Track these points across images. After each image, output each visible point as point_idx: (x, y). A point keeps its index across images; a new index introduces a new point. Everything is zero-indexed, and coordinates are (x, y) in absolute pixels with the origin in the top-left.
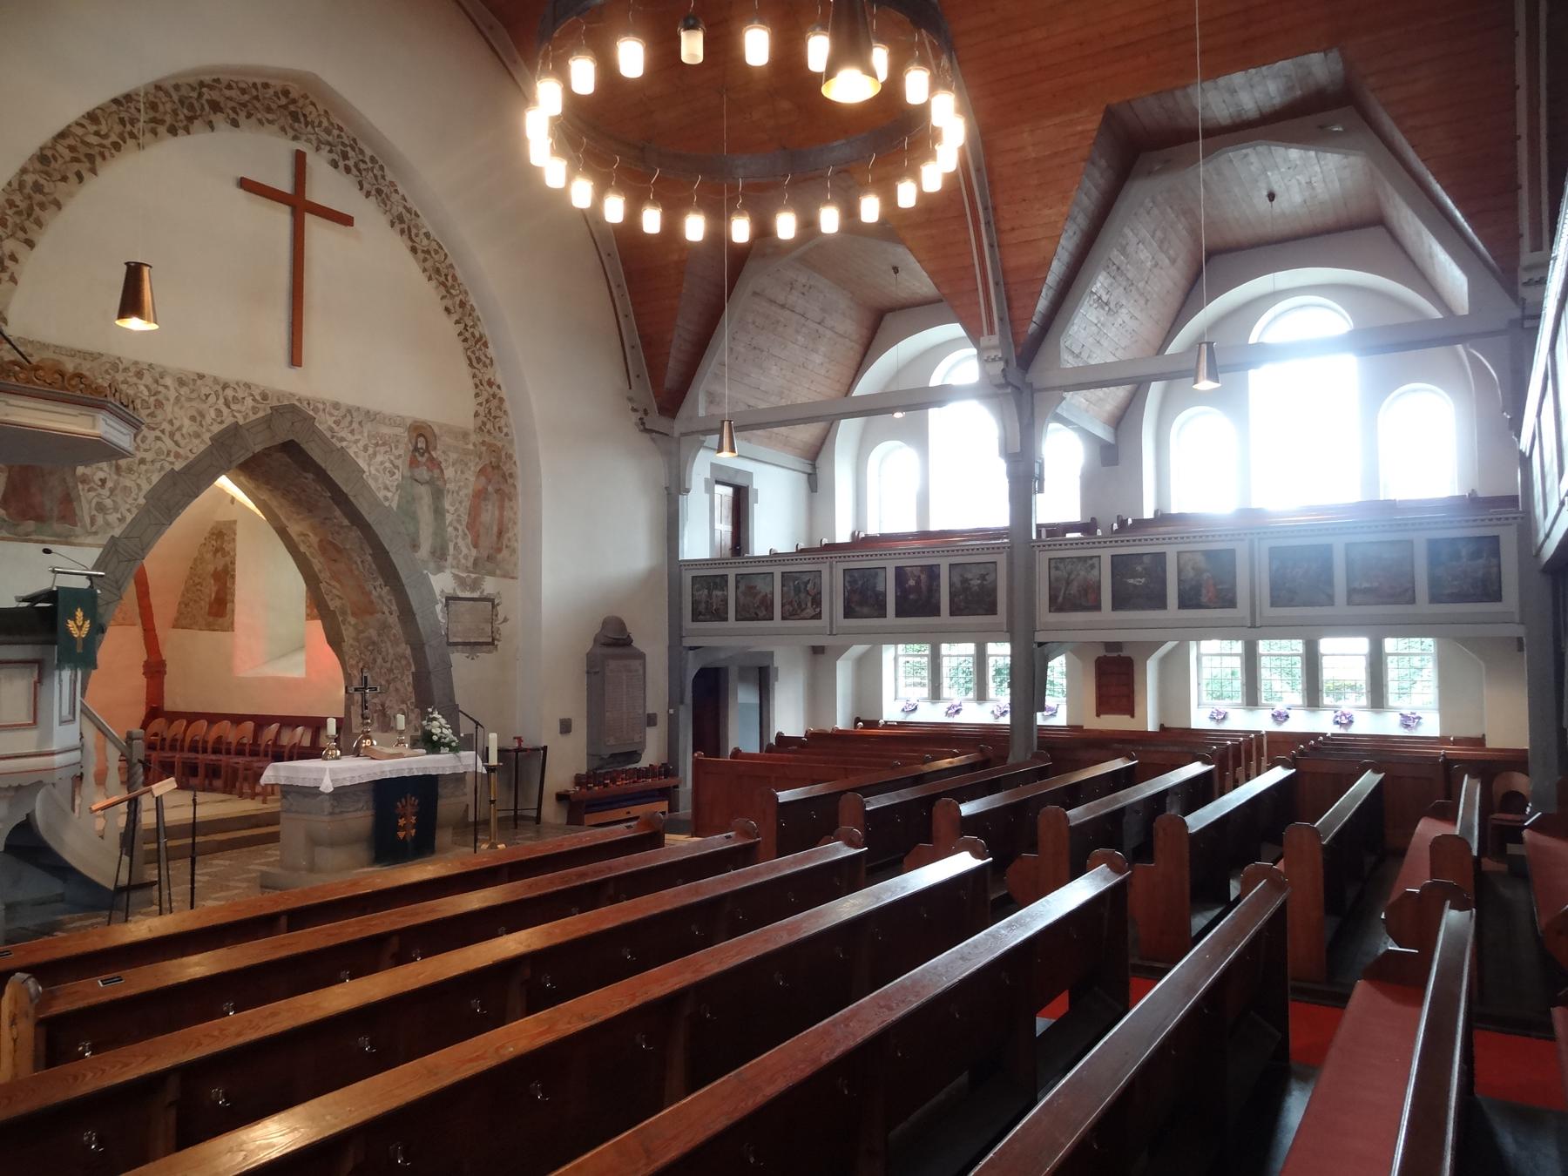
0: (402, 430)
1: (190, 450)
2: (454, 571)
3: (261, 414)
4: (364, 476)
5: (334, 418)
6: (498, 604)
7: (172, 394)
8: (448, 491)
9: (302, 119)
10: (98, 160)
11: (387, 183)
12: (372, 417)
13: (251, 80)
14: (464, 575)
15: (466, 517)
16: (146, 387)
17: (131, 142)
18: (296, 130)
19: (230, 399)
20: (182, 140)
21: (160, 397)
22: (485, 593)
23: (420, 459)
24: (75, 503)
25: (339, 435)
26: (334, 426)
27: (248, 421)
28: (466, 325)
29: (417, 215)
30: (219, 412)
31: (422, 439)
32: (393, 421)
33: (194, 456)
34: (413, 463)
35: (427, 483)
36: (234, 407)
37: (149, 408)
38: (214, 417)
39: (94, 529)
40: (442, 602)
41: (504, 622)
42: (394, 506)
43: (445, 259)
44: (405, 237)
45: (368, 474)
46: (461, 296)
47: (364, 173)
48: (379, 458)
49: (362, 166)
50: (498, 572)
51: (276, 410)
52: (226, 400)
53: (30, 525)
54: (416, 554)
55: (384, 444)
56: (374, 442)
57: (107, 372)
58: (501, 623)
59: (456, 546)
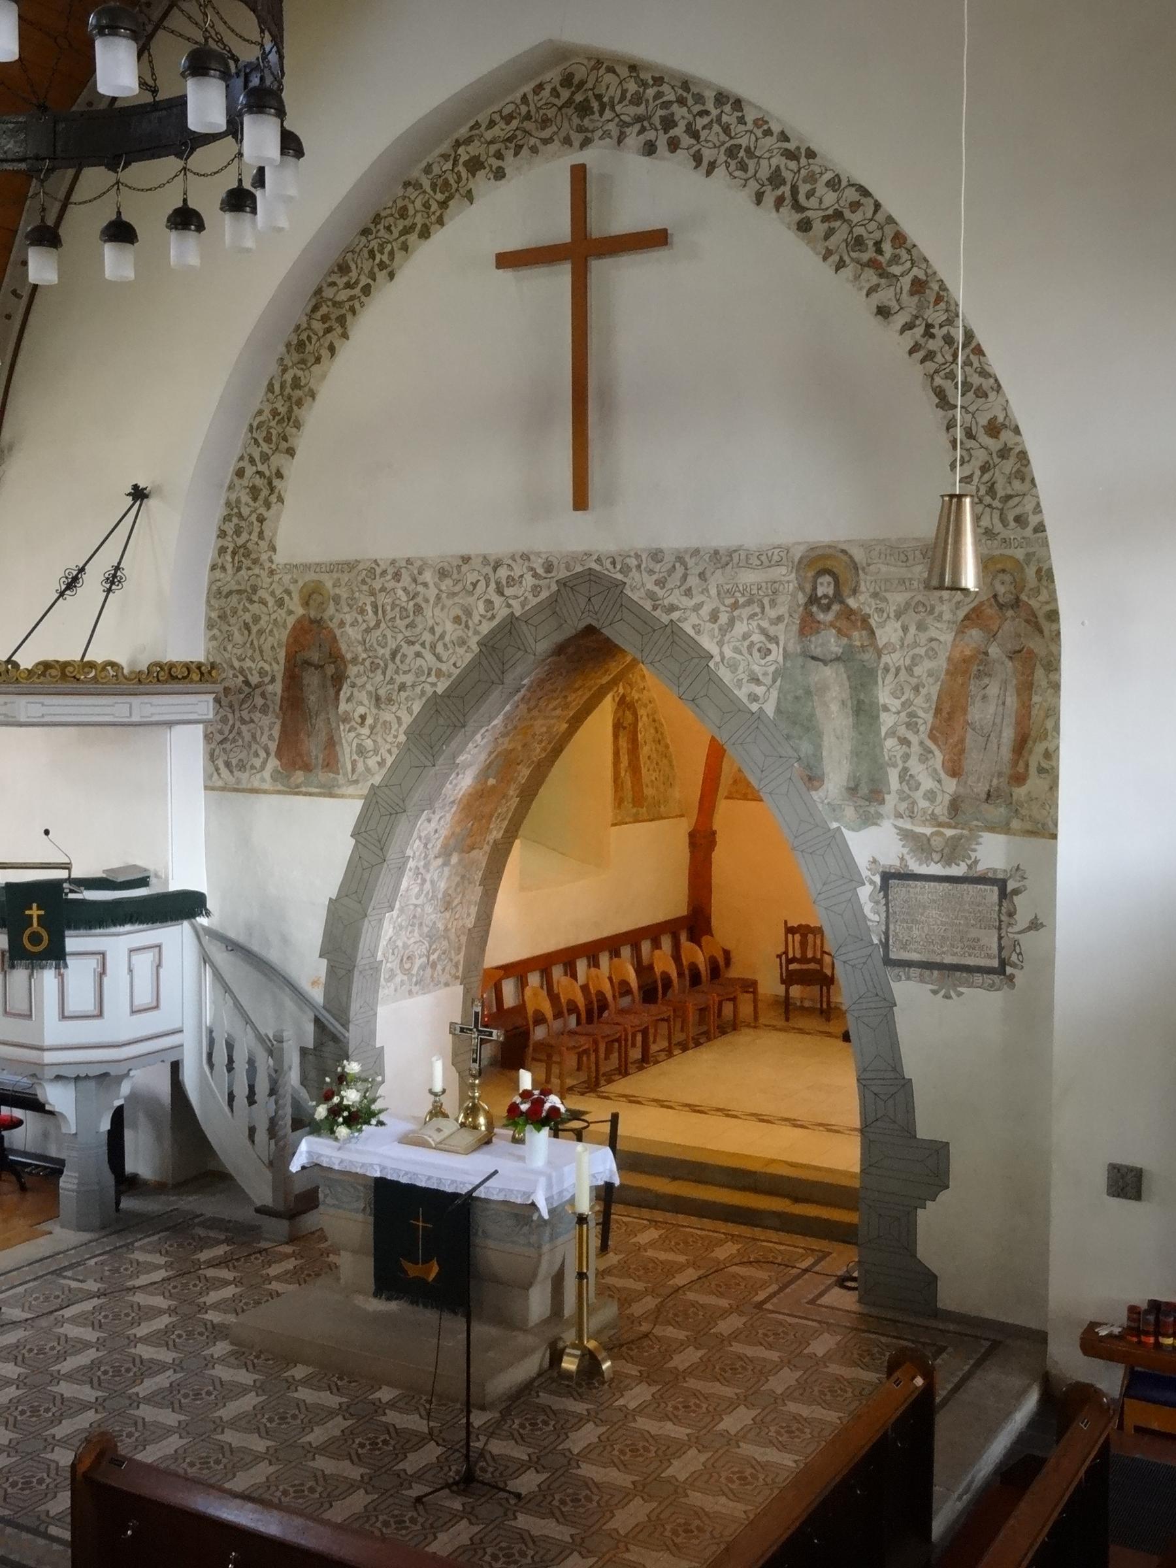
0: (784, 570)
1: (454, 665)
2: (900, 823)
3: (544, 595)
4: (711, 664)
5: (655, 577)
6: (1016, 892)
7: (432, 593)
8: (887, 669)
9: (595, 105)
10: (349, 317)
11: (750, 126)
12: (724, 560)
13: (518, 95)
14: (928, 831)
15: (929, 717)
16: (405, 589)
17: (381, 275)
18: (587, 130)
19: (504, 582)
20: (439, 236)
21: (419, 600)
22: (981, 868)
23: (821, 616)
24: (338, 748)
25: (666, 602)
26: (656, 589)
27: (527, 608)
28: (929, 326)
29: (811, 154)
30: (489, 603)
31: (827, 579)
32: (764, 559)
33: (458, 671)
34: (808, 626)
35: (838, 659)
36: (508, 592)
37: (408, 617)
38: (482, 612)
39: (355, 778)
40: (872, 882)
41: (1029, 929)
42: (770, 709)
43: (875, 212)
44: (786, 210)
45: (717, 658)
46: (915, 271)
47: (704, 134)
48: (740, 628)
49: (701, 122)
50: (1015, 824)
51: (565, 585)
52: (498, 583)
53: (299, 776)
54: (815, 795)
55: (749, 602)
56: (731, 601)
57: (364, 582)
58: (1019, 933)
59: (905, 776)
